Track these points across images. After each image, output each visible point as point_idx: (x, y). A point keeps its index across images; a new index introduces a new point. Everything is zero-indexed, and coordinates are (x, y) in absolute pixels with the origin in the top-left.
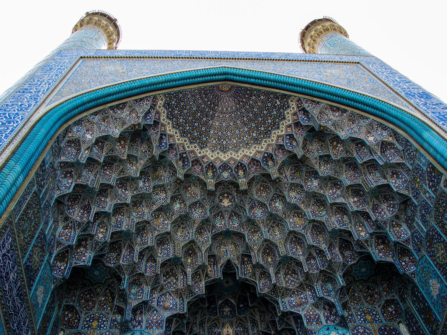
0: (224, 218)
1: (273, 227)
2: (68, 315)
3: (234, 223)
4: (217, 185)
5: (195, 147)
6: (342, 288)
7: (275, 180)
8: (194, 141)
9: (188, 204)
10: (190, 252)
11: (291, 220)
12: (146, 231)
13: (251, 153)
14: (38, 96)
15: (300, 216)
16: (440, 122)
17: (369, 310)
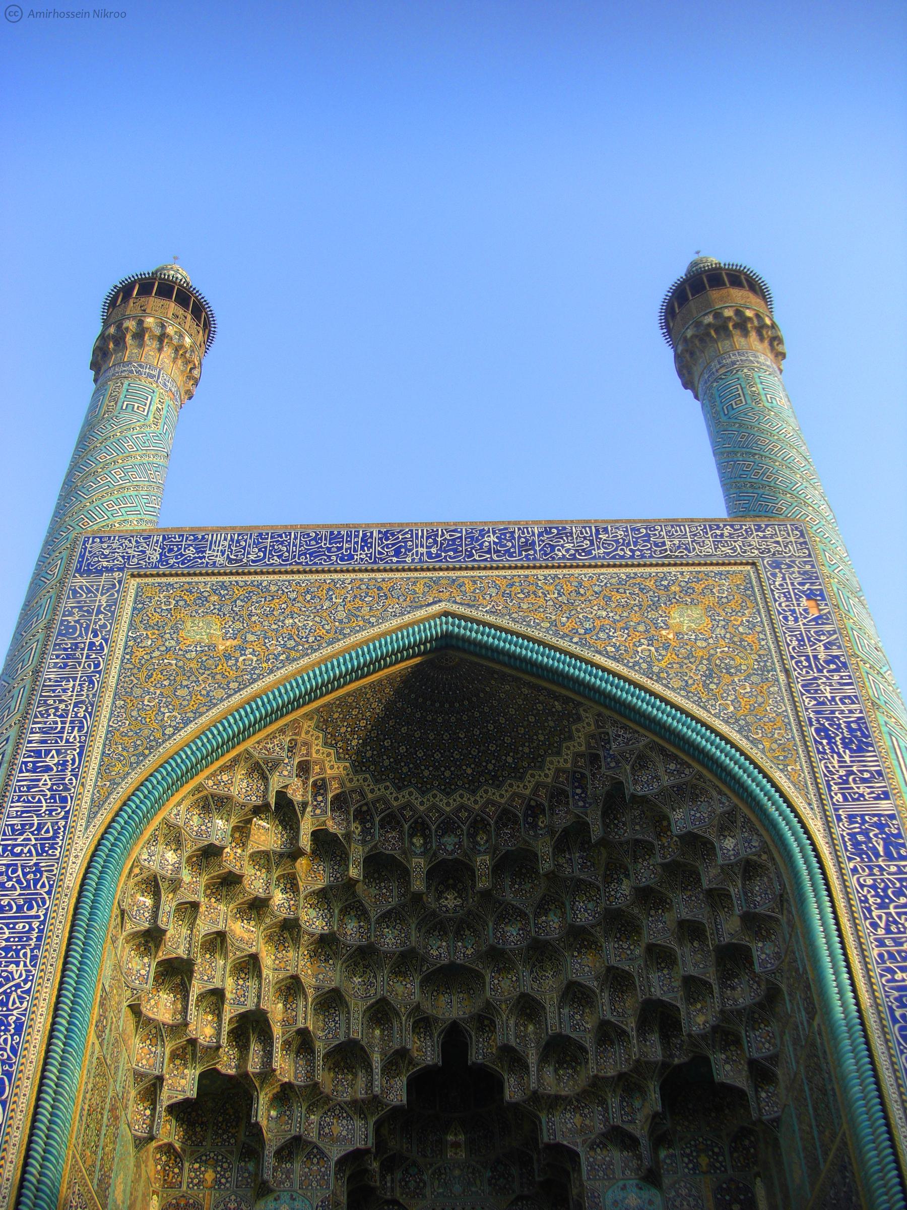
0: (446, 933)
1: (542, 961)
2: (160, 1159)
3: (467, 944)
4: (430, 875)
5: (386, 788)
6: (656, 1115)
7: (546, 875)
8: (384, 777)
9: (373, 916)
10: (380, 1015)
11: (576, 954)
12: (292, 991)
13: (502, 796)
14: (66, 789)
15: (593, 946)
16: (850, 859)
17: (709, 1142)
